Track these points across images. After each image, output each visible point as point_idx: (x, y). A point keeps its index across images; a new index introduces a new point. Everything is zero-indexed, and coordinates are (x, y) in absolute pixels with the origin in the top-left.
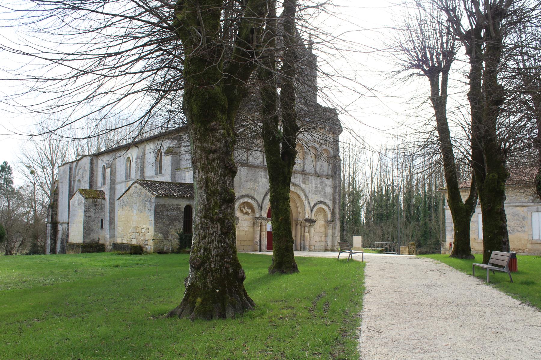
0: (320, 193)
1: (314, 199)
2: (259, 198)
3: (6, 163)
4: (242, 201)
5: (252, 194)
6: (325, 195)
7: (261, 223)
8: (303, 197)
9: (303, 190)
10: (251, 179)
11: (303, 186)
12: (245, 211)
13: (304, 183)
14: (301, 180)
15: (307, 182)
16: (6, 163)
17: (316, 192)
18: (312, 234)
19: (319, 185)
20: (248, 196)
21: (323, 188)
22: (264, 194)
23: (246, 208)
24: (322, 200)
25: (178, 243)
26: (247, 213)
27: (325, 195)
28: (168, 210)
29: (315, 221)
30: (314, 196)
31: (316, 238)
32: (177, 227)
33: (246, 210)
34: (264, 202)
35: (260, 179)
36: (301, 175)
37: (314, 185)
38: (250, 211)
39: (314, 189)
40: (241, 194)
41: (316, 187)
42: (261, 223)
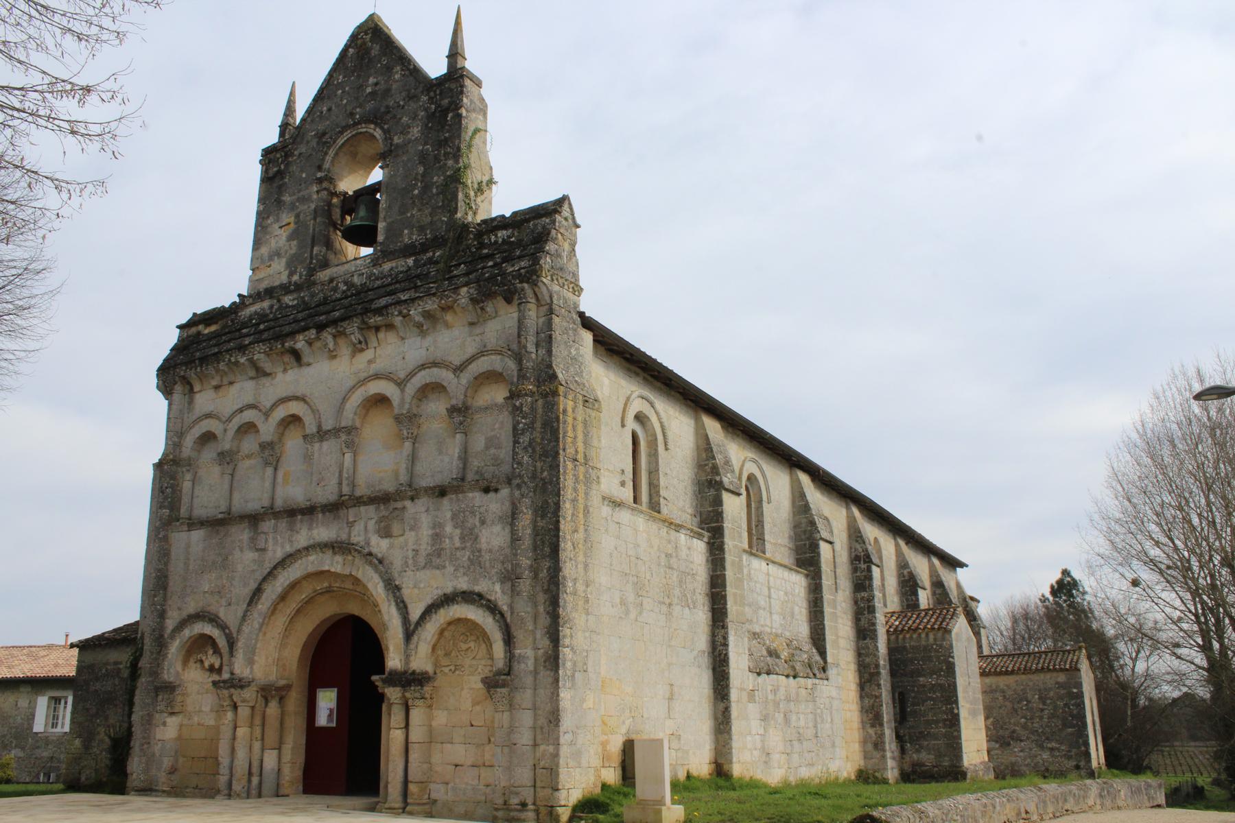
1: (421, 588)
3: (1065, 573)
4: (187, 633)
6: (476, 561)
9: (378, 562)
10: (214, 563)
11: (380, 545)
13: (386, 533)
16: (1065, 573)
17: (435, 558)
18: (416, 734)
19: (449, 529)
20: (198, 617)
21: (470, 536)
24: (463, 584)
25: (108, 762)
28: (97, 679)
30: (424, 575)
31: (459, 752)
32: (111, 721)
36: (372, 508)
37: (426, 532)
39: (425, 548)
40: (185, 614)
41: (437, 537)
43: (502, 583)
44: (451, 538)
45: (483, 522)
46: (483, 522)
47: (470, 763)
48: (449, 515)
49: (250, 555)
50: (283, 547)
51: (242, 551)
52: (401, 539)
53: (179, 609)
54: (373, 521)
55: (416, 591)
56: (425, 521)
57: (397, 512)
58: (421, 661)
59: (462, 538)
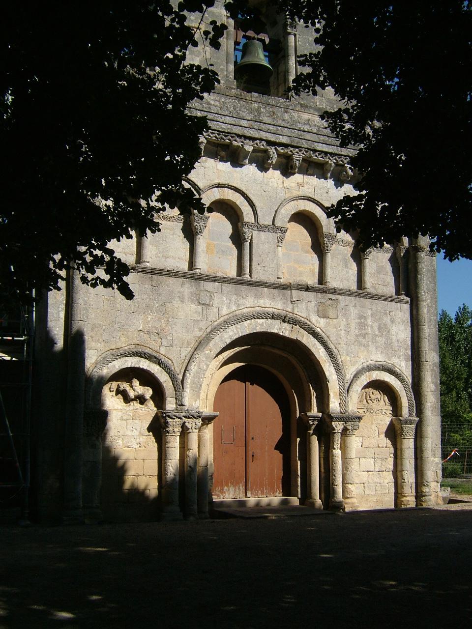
0: (374, 340)
2: (176, 357)
5: (152, 345)
7: (183, 426)
8: (320, 353)
12: (132, 394)
14: (312, 306)
15: (331, 313)
19: (369, 321)
22: (193, 344)
23: (136, 383)
24: (379, 358)
26: (141, 399)
27: (388, 347)
29: (360, 418)
33: (137, 388)
34: (193, 368)
35: (177, 303)
38: (148, 392)
42: (183, 426)
43: (406, 361)
44: (372, 327)
45: (392, 322)
46: (392, 322)
47: (377, 470)
48: (370, 312)
49: (194, 307)
50: (229, 307)
51: (182, 301)
52: (335, 321)
53: (106, 342)
54: (313, 304)
55: (348, 358)
56: (354, 312)
57: (330, 301)
58: (353, 407)
59: (380, 328)
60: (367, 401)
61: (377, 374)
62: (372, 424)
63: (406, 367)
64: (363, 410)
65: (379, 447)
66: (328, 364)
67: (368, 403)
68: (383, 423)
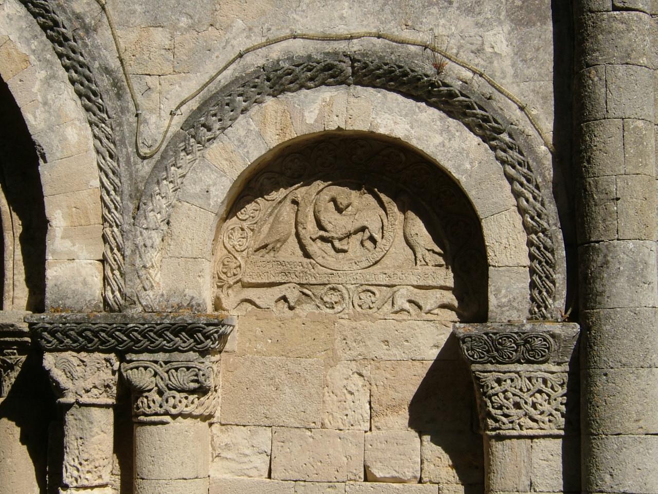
43: (518, 23)
55: (160, 37)
60: (303, 247)
61: (330, 104)
62: (332, 360)
63: (519, 53)
64: (277, 292)
65: (368, 477)
66: (42, 74)
67: (307, 255)
68: (397, 353)
